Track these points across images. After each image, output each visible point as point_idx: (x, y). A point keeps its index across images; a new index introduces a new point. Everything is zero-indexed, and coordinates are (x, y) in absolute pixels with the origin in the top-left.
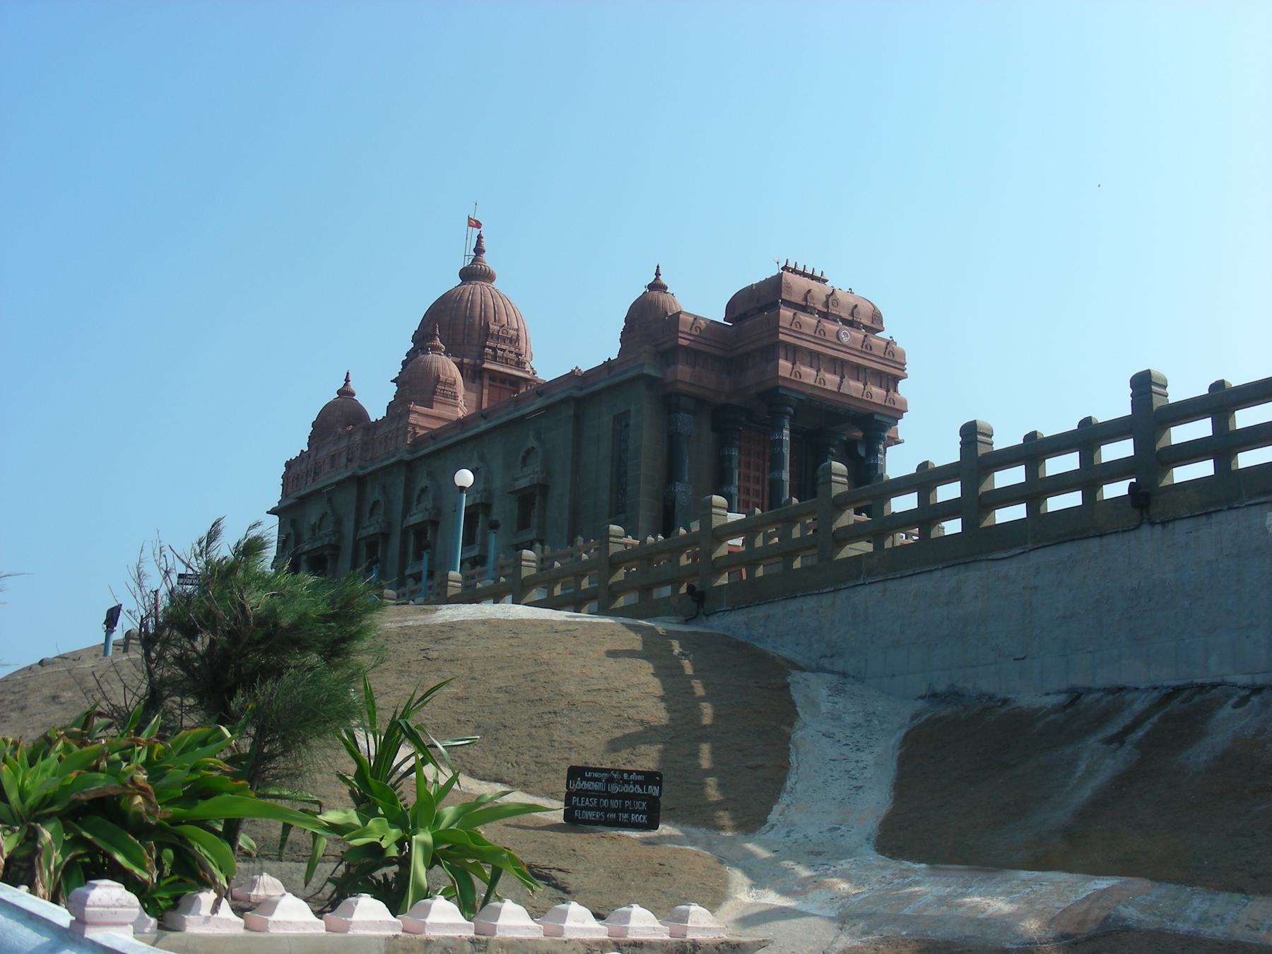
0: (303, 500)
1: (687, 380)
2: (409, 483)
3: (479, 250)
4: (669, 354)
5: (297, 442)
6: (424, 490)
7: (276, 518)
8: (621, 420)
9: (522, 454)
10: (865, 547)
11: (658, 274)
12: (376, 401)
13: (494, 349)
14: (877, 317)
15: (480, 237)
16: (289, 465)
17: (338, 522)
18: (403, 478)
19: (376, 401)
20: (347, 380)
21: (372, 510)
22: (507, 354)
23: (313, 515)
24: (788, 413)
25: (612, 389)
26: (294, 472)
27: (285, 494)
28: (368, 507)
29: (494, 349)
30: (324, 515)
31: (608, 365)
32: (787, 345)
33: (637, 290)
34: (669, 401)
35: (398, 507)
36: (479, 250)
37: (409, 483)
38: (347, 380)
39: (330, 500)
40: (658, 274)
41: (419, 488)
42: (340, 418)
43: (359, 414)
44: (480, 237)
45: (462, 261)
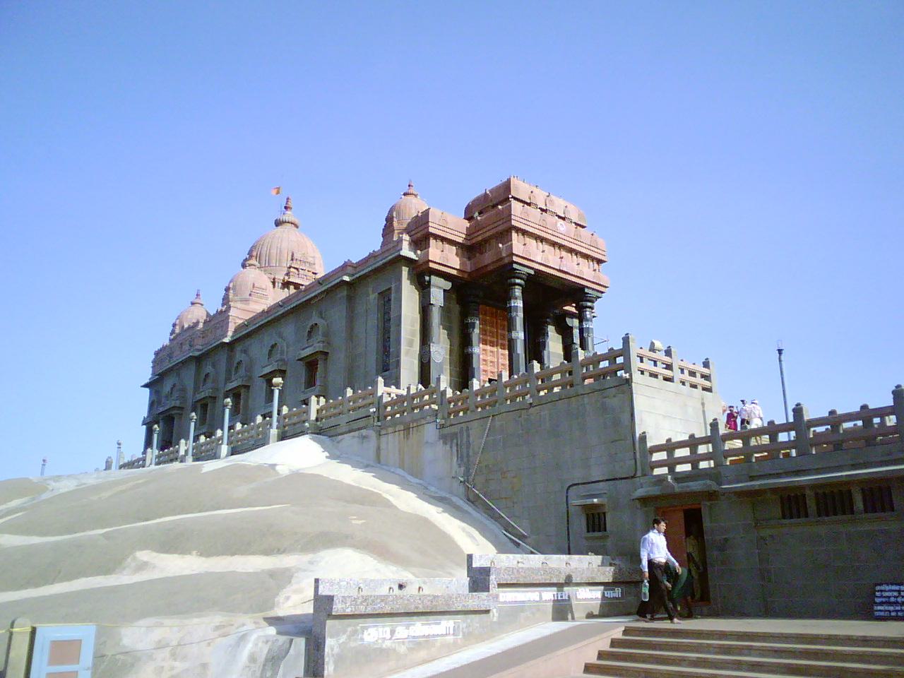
2: (230, 358)
6: (240, 363)
7: (147, 390)
9: (308, 329)
13: (297, 269)
16: (157, 354)
18: (225, 356)
21: (205, 380)
22: (306, 273)
23: (167, 387)
24: (519, 284)
25: (377, 271)
26: (160, 356)
28: (203, 376)
29: (297, 269)
30: (174, 385)
31: (373, 256)
35: (222, 377)
37: (230, 358)
39: (178, 375)
41: (236, 362)
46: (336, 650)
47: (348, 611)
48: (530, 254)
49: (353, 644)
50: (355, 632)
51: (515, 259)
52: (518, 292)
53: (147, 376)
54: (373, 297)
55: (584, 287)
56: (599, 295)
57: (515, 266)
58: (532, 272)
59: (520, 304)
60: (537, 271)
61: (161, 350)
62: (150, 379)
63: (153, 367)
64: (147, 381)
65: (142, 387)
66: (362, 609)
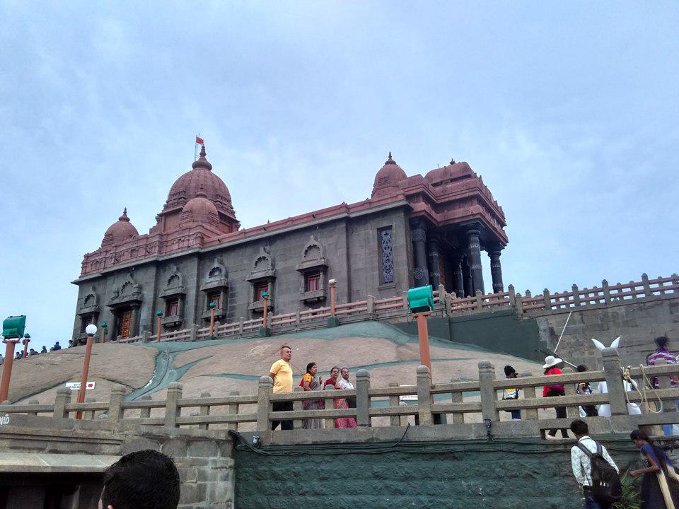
0: (105, 276)
3: (203, 154)
5: (94, 243)
10: (630, 297)
11: (390, 157)
12: (144, 223)
15: (203, 147)
17: (140, 288)
19: (144, 223)
20: (125, 212)
27: (84, 273)
31: (368, 202)
33: (380, 165)
36: (203, 154)
38: (125, 212)
40: (390, 157)
42: (121, 234)
43: (132, 232)
44: (203, 147)
53: (77, 274)
61: (95, 254)
62: (80, 277)
63: (82, 268)
64: (77, 278)
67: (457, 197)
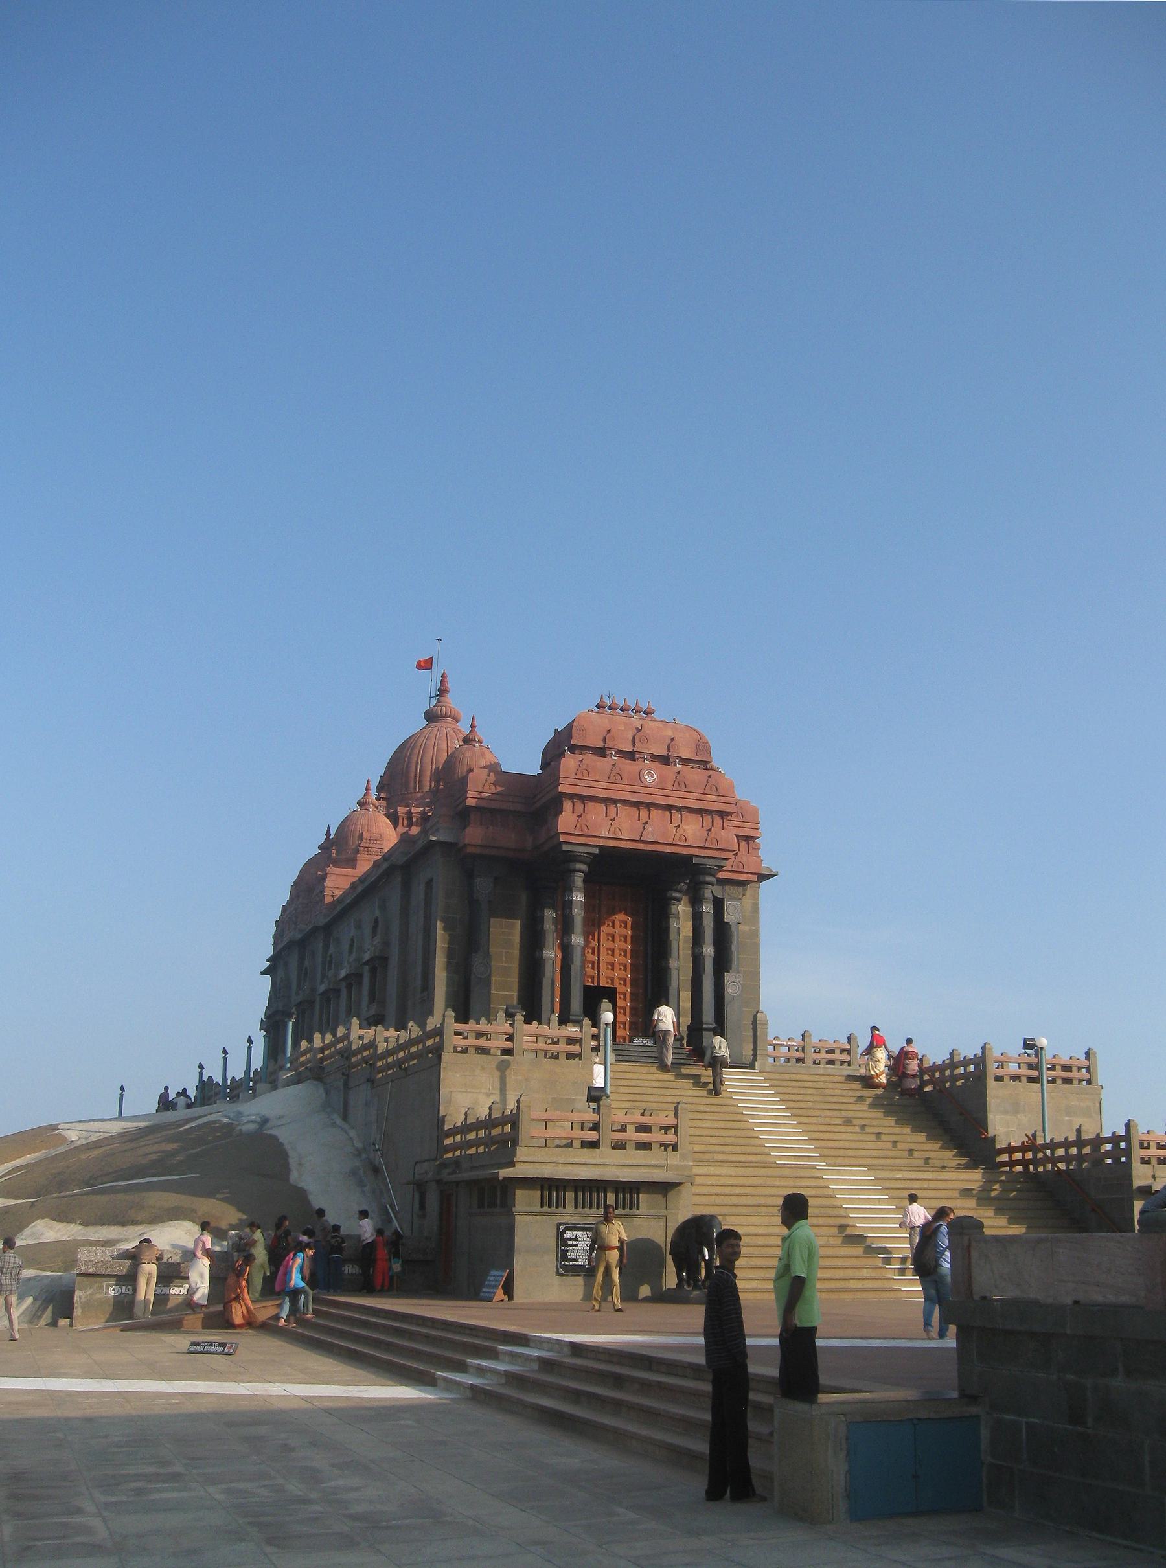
1: (479, 843)
4: (464, 815)
8: (429, 883)
14: (702, 746)
32: (572, 797)
34: (467, 863)
45: (428, 703)
46: (83, 1299)
47: (90, 1271)
48: (586, 827)
49: (98, 1296)
50: (101, 1288)
51: (562, 838)
52: (579, 880)
54: (422, 887)
55: (691, 857)
56: (718, 863)
57: (565, 847)
58: (596, 851)
59: (578, 897)
60: (601, 848)
65: (262, 973)
66: (102, 1271)
67: (544, 800)
